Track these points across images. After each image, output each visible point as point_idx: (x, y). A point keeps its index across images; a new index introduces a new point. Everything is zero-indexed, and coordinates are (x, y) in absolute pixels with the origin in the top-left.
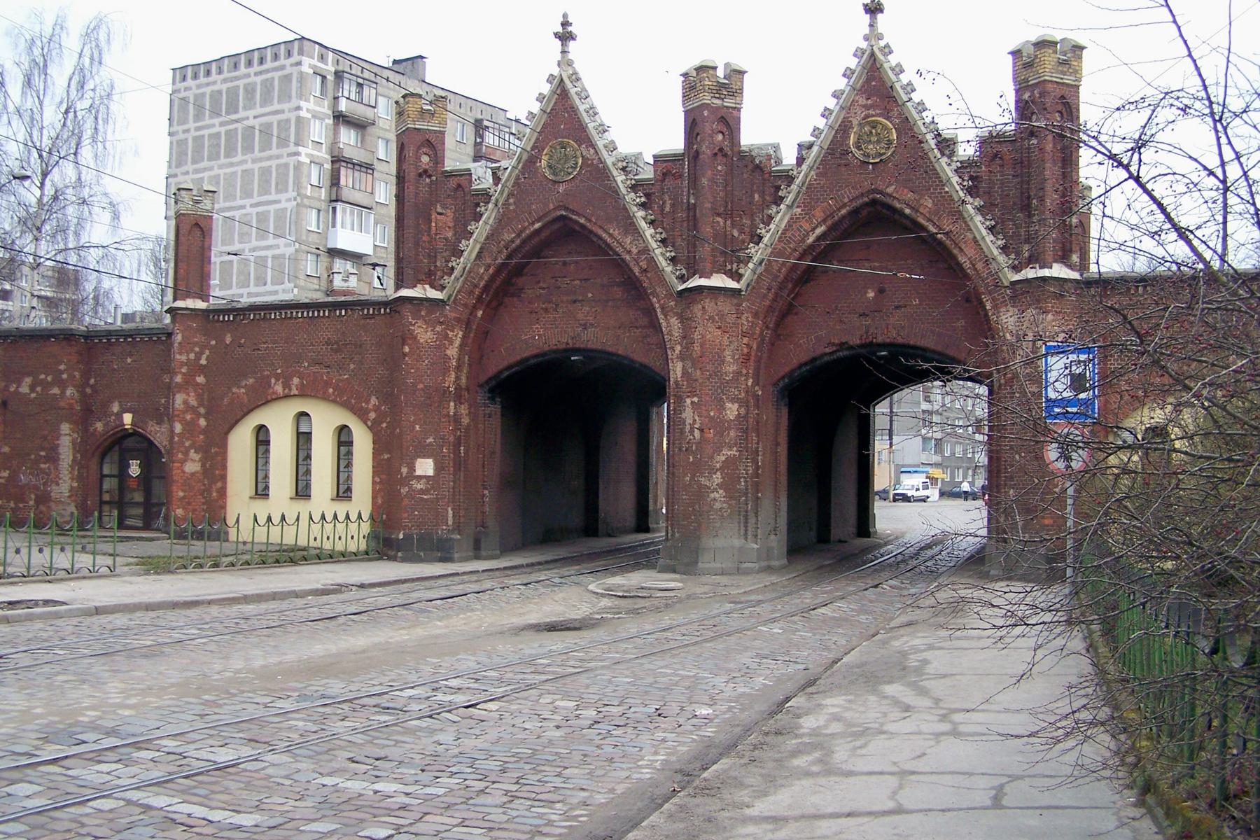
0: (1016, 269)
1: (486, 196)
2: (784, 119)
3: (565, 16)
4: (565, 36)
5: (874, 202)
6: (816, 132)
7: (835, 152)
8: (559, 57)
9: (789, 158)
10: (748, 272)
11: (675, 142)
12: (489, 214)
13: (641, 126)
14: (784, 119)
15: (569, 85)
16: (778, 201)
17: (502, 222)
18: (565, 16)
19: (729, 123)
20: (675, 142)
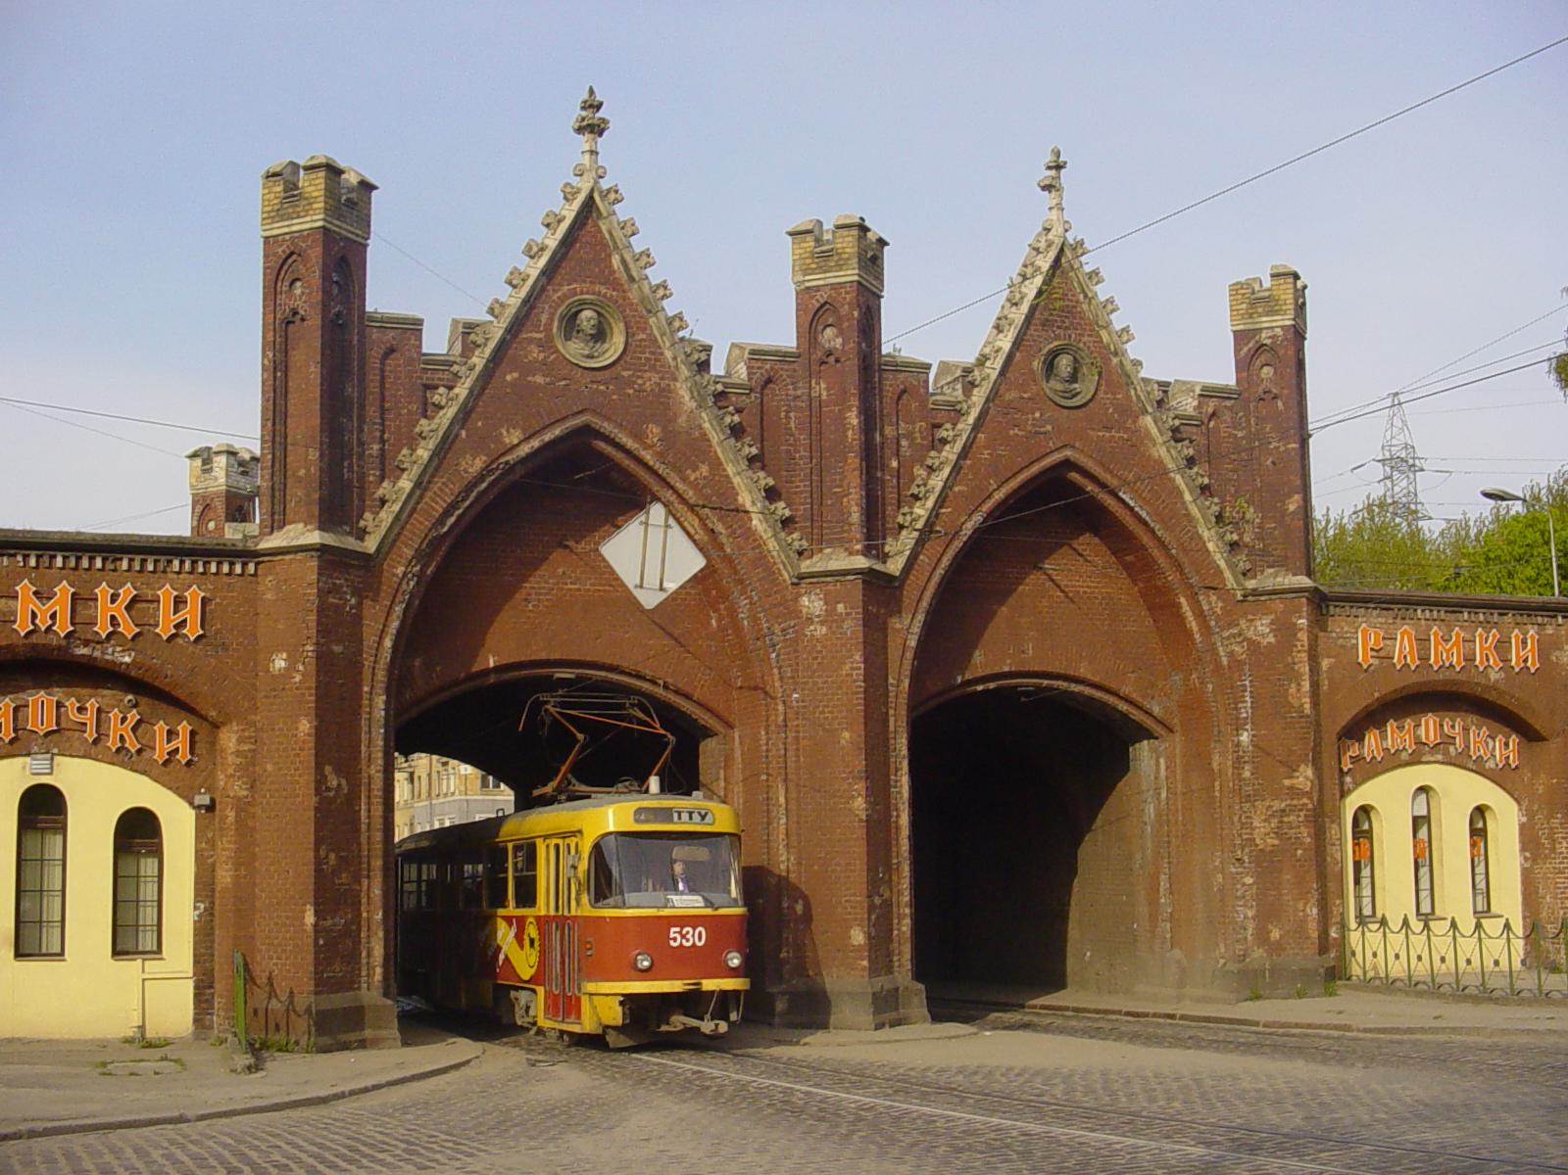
1: (440, 371)
2: (944, 321)
11: (784, 336)
13: (731, 301)
14: (944, 321)
20: (784, 336)
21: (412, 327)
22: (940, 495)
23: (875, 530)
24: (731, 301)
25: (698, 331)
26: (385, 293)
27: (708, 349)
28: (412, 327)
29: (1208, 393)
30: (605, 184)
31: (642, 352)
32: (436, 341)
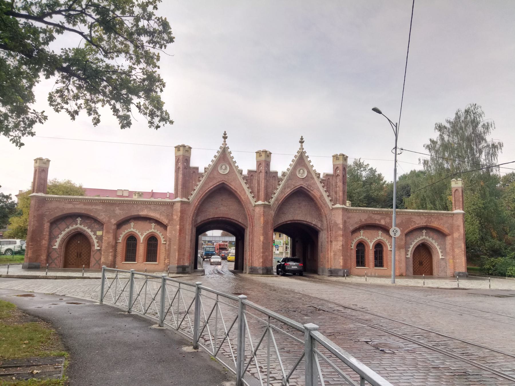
0: (333, 205)
1: (201, 175)
2: (281, 165)
3: (225, 132)
4: (225, 138)
5: (301, 187)
6: (288, 169)
7: (292, 174)
8: (223, 142)
9: (280, 175)
10: (272, 201)
11: (254, 168)
12: (203, 180)
13: (246, 163)
14: (281, 165)
15: (226, 149)
16: (279, 185)
17: (205, 183)
18: (225, 132)
19: (268, 164)
20: (254, 168)
21: (197, 168)
22: (279, 193)
23: (267, 197)
24: (246, 163)
25: (240, 168)
26: (193, 163)
27: (242, 171)
28: (197, 168)
29: (327, 175)
30: (227, 146)
31: (232, 171)
32: (201, 170)
